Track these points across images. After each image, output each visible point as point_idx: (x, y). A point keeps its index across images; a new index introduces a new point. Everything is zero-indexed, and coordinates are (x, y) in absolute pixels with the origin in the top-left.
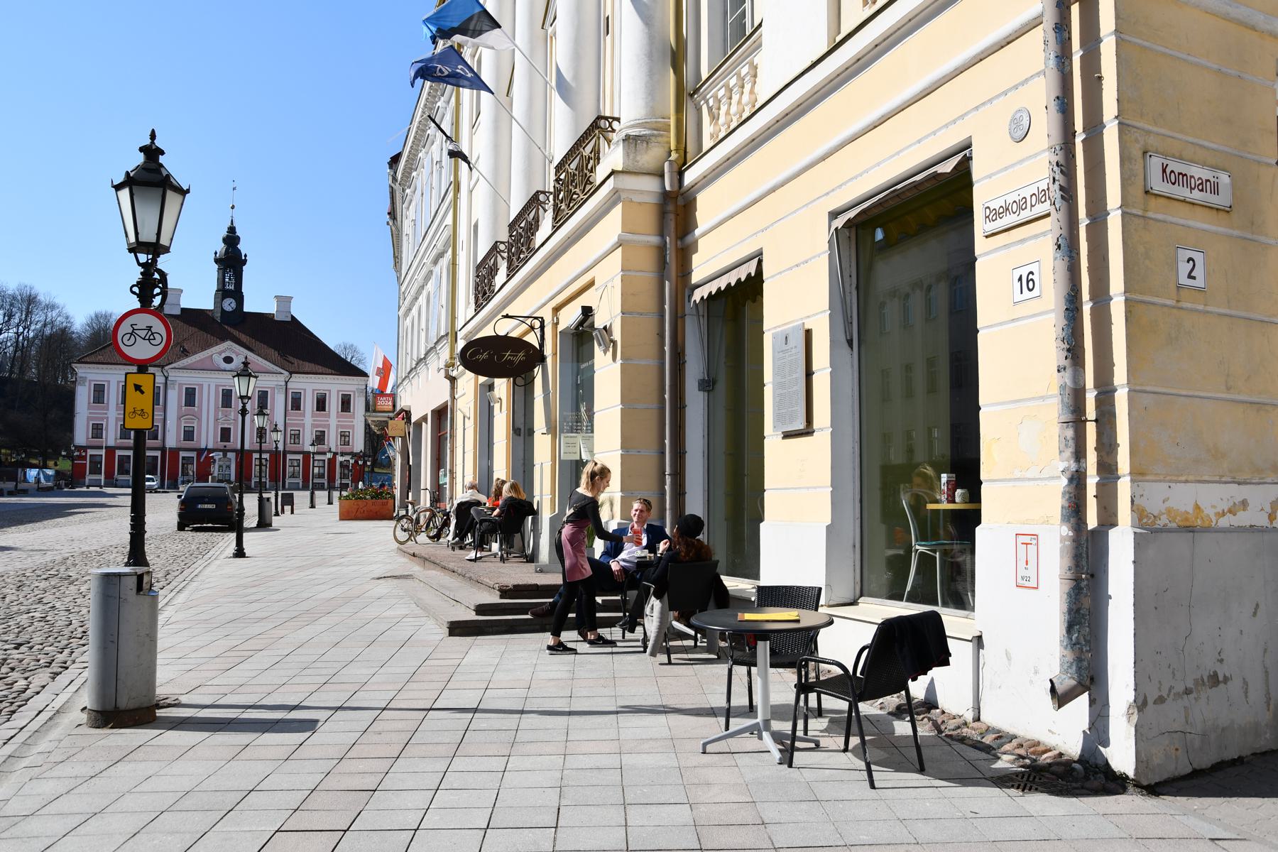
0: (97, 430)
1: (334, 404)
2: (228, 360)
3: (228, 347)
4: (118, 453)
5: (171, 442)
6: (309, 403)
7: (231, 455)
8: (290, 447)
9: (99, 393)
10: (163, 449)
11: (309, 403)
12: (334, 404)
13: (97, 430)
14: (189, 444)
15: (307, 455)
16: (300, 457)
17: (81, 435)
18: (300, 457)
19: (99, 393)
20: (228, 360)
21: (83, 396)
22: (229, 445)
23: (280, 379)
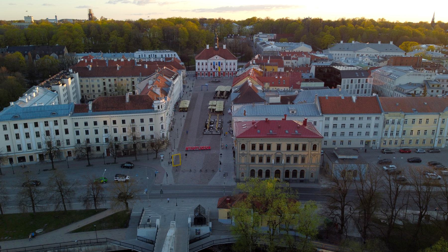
0: (199, 69)
1: (232, 64)
2: (217, 58)
3: (217, 56)
4: (206, 72)
5: (209, 71)
6: (229, 64)
7: (218, 72)
8: (226, 71)
9: (199, 64)
10: (208, 72)
11: (229, 64)
12: (232, 64)
13: (199, 69)
14: (211, 71)
15: (228, 72)
16: (228, 72)
17: (197, 70)
18: (228, 72)
19: (199, 64)
20: (217, 58)
21: (197, 64)
22: (217, 71)
23: (224, 61)
